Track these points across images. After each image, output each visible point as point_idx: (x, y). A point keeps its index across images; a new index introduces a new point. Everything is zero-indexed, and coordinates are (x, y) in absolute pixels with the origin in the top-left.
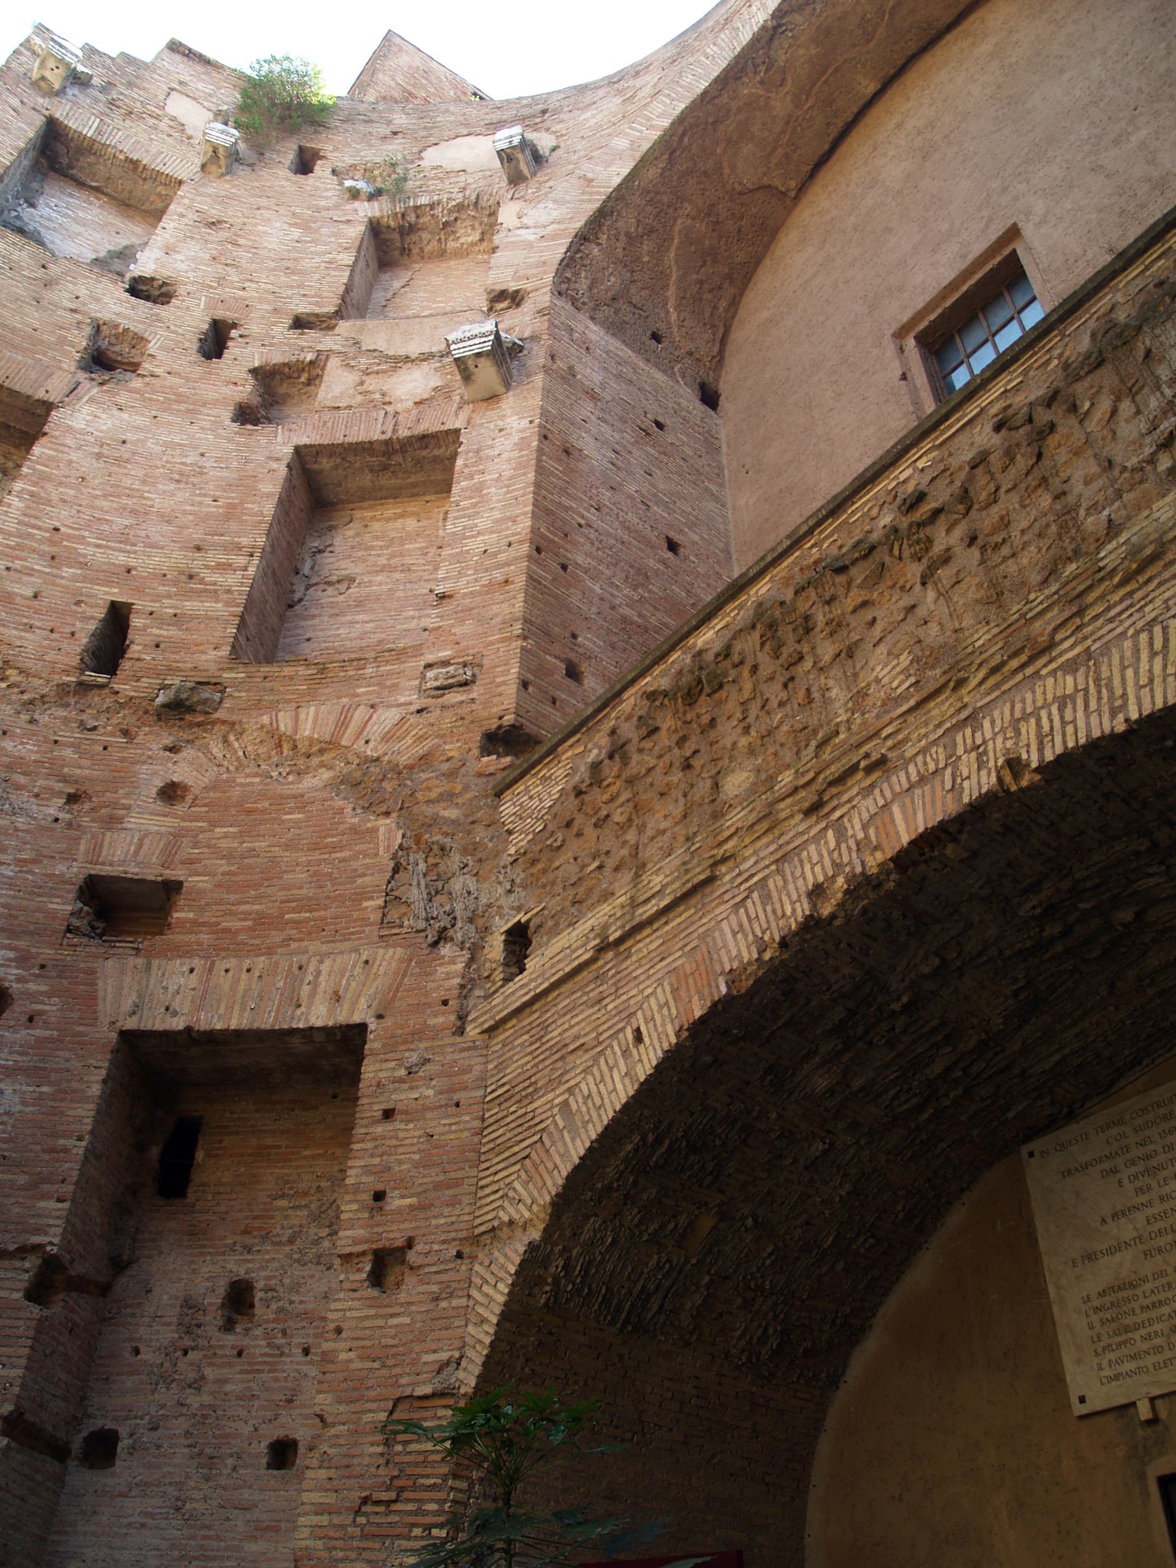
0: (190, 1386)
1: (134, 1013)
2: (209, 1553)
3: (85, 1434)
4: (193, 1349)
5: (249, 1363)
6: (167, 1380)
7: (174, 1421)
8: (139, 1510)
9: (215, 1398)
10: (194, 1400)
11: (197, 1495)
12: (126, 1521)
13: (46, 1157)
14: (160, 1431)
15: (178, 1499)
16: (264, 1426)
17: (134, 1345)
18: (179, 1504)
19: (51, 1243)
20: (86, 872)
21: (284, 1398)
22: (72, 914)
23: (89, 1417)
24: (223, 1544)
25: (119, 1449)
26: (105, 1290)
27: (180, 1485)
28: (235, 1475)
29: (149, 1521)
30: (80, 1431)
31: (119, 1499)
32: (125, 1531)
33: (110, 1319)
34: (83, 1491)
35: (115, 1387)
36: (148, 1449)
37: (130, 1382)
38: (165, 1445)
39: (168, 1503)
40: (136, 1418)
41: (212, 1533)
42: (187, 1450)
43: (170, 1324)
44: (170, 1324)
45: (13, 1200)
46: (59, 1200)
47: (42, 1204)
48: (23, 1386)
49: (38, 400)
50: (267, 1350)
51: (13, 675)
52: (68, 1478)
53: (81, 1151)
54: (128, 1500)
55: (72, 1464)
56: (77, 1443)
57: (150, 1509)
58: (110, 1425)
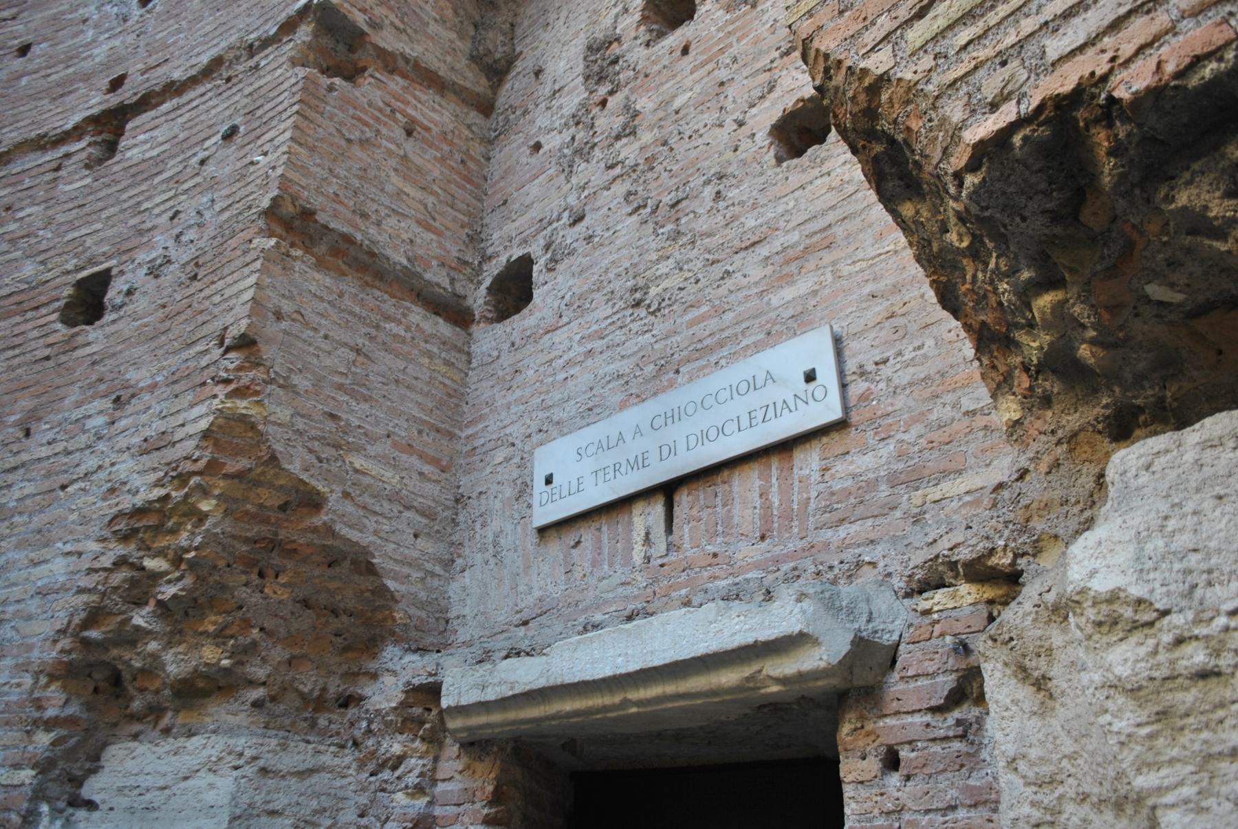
0: (618, 138)
2: (708, 342)
3: (487, 282)
4: (612, 93)
5: (702, 53)
6: (583, 152)
7: (606, 193)
8: (578, 337)
9: (660, 127)
10: (629, 151)
11: (663, 268)
12: (561, 362)
14: (587, 219)
15: (635, 290)
16: (754, 111)
17: (532, 143)
18: (638, 295)
21: (777, 54)
23: (490, 258)
24: (729, 316)
25: (535, 275)
26: (486, 108)
27: (632, 271)
28: (722, 204)
29: (598, 344)
30: (480, 283)
31: (548, 336)
32: (562, 376)
33: (496, 137)
34: (495, 353)
35: (516, 206)
36: (575, 250)
37: (534, 189)
38: (599, 232)
39: (621, 304)
40: (550, 223)
41: (704, 309)
42: (635, 217)
43: (575, 88)
44: (575, 88)
48: (289, 163)
50: (728, 17)
52: (473, 347)
54: (558, 332)
55: (478, 330)
56: (478, 298)
57: (595, 327)
58: (517, 253)
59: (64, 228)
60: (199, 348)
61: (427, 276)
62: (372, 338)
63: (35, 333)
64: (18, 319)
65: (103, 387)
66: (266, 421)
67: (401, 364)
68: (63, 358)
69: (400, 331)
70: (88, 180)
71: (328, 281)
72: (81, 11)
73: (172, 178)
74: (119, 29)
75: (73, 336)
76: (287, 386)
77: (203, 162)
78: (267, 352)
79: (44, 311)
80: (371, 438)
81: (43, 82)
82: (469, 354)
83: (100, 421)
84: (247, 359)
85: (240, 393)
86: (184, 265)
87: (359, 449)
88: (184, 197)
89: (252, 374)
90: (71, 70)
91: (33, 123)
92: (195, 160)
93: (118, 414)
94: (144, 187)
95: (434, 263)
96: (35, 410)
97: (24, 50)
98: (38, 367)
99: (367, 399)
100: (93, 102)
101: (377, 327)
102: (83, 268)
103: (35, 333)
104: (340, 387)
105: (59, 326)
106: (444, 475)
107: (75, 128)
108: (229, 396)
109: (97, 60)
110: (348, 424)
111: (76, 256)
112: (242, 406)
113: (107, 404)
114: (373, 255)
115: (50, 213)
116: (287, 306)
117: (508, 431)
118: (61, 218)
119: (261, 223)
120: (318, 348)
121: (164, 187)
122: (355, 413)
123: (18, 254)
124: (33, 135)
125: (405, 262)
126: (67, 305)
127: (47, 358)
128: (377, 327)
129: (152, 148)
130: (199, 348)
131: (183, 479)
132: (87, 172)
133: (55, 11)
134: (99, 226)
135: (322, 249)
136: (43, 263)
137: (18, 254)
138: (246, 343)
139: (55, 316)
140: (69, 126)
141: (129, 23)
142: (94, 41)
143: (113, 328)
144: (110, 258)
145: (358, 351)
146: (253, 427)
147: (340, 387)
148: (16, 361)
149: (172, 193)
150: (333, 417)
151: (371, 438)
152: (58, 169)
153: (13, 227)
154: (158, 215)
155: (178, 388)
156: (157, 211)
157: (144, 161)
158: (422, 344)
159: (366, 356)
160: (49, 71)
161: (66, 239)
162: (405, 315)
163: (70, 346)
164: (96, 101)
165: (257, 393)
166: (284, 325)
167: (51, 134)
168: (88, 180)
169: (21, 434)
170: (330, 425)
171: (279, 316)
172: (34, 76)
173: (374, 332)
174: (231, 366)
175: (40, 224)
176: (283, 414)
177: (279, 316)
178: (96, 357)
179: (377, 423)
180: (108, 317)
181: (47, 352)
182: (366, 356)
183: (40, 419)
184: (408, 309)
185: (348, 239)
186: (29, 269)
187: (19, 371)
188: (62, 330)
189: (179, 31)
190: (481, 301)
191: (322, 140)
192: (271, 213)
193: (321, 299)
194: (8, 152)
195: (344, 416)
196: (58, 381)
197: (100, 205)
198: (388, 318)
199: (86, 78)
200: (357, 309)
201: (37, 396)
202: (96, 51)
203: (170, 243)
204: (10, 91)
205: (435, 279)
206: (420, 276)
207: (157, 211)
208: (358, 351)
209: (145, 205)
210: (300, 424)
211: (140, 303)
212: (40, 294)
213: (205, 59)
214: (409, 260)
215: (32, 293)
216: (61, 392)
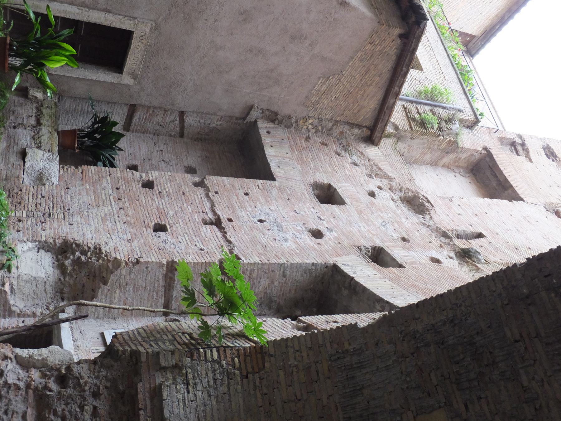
1: (345, 265)
13: (274, 255)
19: (243, 261)
20: (382, 246)
22: (364, 246)
45: (252, 251)
46: (260, 261)
47: (256, 257)
49: (520, 197)
51: (427, 217)
53: (282, 262)
59: (183, 218)
60: (139, 253)
61: (173, 302)
62: (150, 290)
63: (152, 218)
64: (157, 213)
65: (134, 236)
66: (121, 269)
67: (146, 299)
68: (143, 226)
69: (155, 298)
70: (197, 220)
71: (161, 277)
72: (259, 205)
73: (193, 239)
74: (250, 216)
75: (150, 227)
76: (130, 273)
77: (196, 245)
78: (137, 267)
79: (158, 219)
80: (124, 294)
81: (234, 202)
82: (156, 316)
83: (125, 237)
84: (134, 263)
85: (126, 263)
86: (164, 247)
87: (121, 291)
88: (186, 243)
89: (131, 264)
90: (237, 208)
91: (220, 203)
92: (197, 243)
93: (126, 241)
94: (192, 233)
95: (178, 303)
96: (130, 223)
97: (246, 194)
98: (142, 221)
99: (134, 291)
100: (225, 216)
101: (153, 291)
102: (169, 225)
103: (152, 218)
104: (135, 285)
105: (153, 223)
106: (121, 314)
107: (216, 213)
108: (125, 261)
109: (240, 213)
110: (126, 288)
111: (174, 223)
112: (124, 264)
113: (129, 238)
114: (173, 287)
115: (189, 214)
116: (150, 269)
117: (132, 326)
118: (186, 217)
119: (170, 260)
120: (142, 278)
121: (190, 238)
122: (130, 289)
123: (177, 209)
124: (215, 204)
125: (174, 295)
126: (159, 224)
127: (145, 223)
128: (153, 291)
129: (204, 233)
130: (139, 253)
131: (106, 256)
132: (201, 220)
133: (261, 198)
134: (182, 226)
135: (170, 275)
136: (173, 216)
137: (177, 209)
138: (138, 262)
139: (156, 222)
140: (217, 212)
141: (252, 219)
142: (247, 211)
143: (150, 235)
144: (171, 230)
145: (145, 287)
146: (119, 267)
147: (135, 285)
148: (145, 216)
149: (187, 240)
150: (127, 284)
151: (124, 294)
152: (203, 212)
153: (185, 206)
154: (181, 239)
155: (130, 251)
156: (183, 238)
157: (201, 232)
158: (154, 303)
159: (145, 290)
160: (238, 203)
161: (179, 219)
162: (160, 298)
163: (147, 227)
164: (223, 217)
165: (127, 266)
166: (145, 269)
167: (215, 208)
168: (197, 220)
169: (124, 222)
170: (125, 284)
171: (147, 268)
172: (236, 199)
173: (152, 290)
174: (132, 260)
175: (185, 212)
176: (124, 273)
177: (147, 268)
178: (142, 233)
179: (129, 295)
180: (153, 233)
181: (146, 222)
182: (145, 290)
183: (128, 225)
184: (162, 298)
185: (174, 280)
186: (171, 213)
187: (142, 218)
188: (152, 225)
189: (245, 231)
190: (172, 317)
191: (198, 269)
192: (173, 262)
193: (155, 277)
194: (210, 199)
195: (128, 286)
196: (137, 227)
197: (189, 225)
198: (157, 293)
199: (234, 212)
200: (156, 285)
201: (134, 223)
202: (243, 213)
203: (172, 242)
204: (232, 194)
205: (174, 305)
206: (172, 300)
207: (183, 238)
208: (145, 287)
209: (186, 235)
210: (123, 277)
211: (156, 240)
212: (164, 217)
213: (232, 239)
214: (175, 296)
215: (164, 215)
216: (134, 228)
